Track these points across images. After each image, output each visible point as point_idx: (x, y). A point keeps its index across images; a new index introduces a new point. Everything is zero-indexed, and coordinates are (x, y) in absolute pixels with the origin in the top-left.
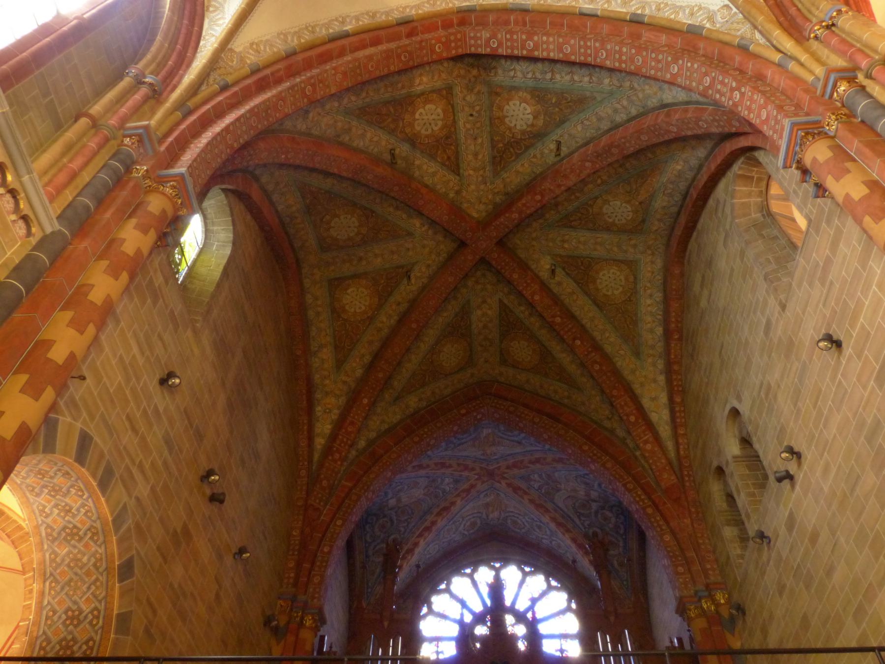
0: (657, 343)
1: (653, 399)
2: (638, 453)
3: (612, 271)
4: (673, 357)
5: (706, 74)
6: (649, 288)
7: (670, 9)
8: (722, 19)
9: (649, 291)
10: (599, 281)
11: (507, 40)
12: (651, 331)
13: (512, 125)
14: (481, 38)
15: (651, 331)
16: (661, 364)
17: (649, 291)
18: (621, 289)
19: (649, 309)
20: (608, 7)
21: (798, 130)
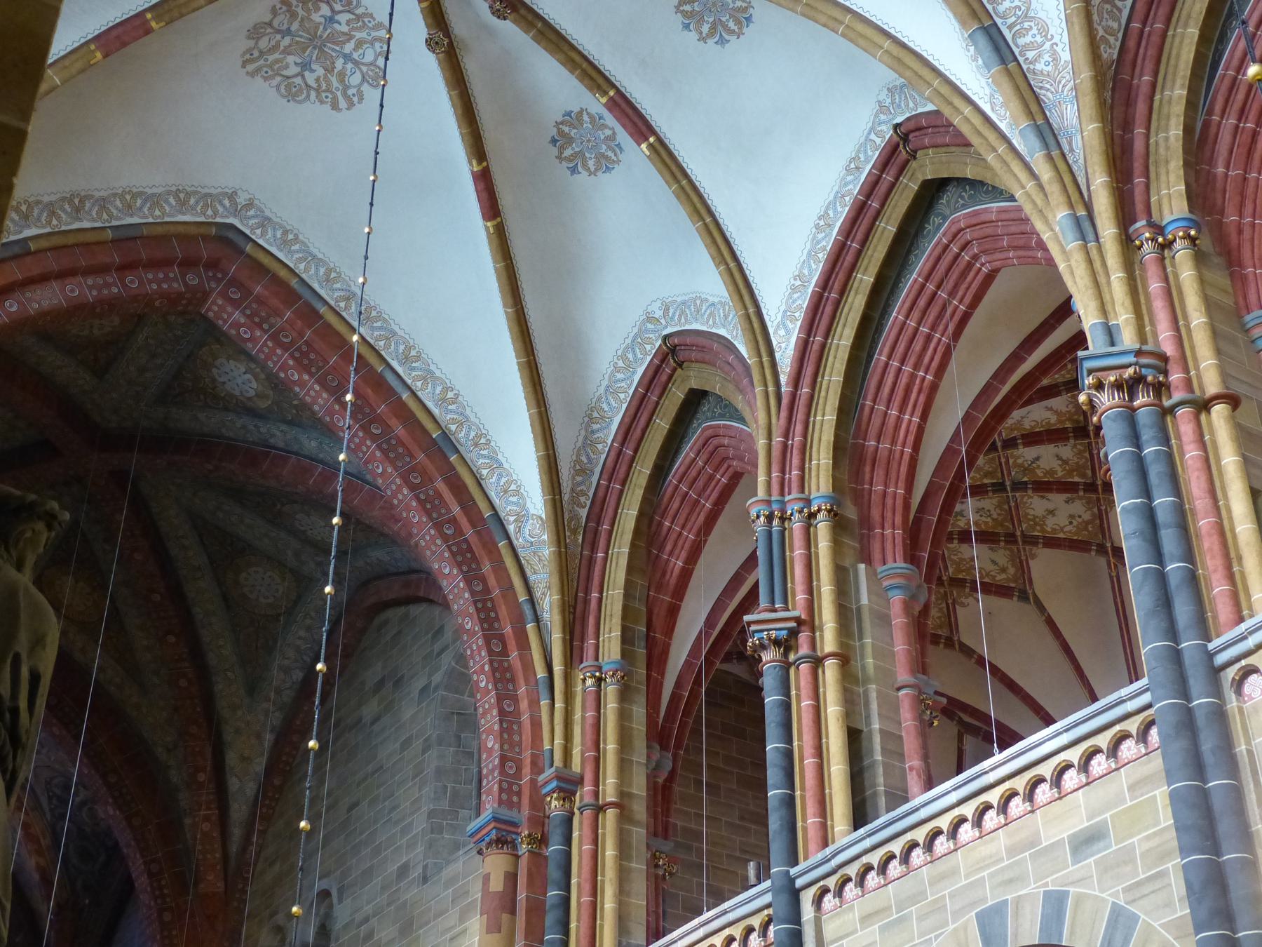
0: (286, 689)
1: (245, 759)
2: (188, 821)
3: (269, 573)
4: (298, 722)
5: (470, 616)
6: (312, 618)
7: (488, 457)
8: (529, 535)
9: (308, 621)
10: (244, 575)
11: (265, 344)
12: (286, 670)
13: (221, 380)
14: (230, 315)
15: (286, 670)
16: (276, 718)
17: (308, 621)
18: (271, 600)
19: (299, 642)
20: (421, 389)
21: (494, 828)
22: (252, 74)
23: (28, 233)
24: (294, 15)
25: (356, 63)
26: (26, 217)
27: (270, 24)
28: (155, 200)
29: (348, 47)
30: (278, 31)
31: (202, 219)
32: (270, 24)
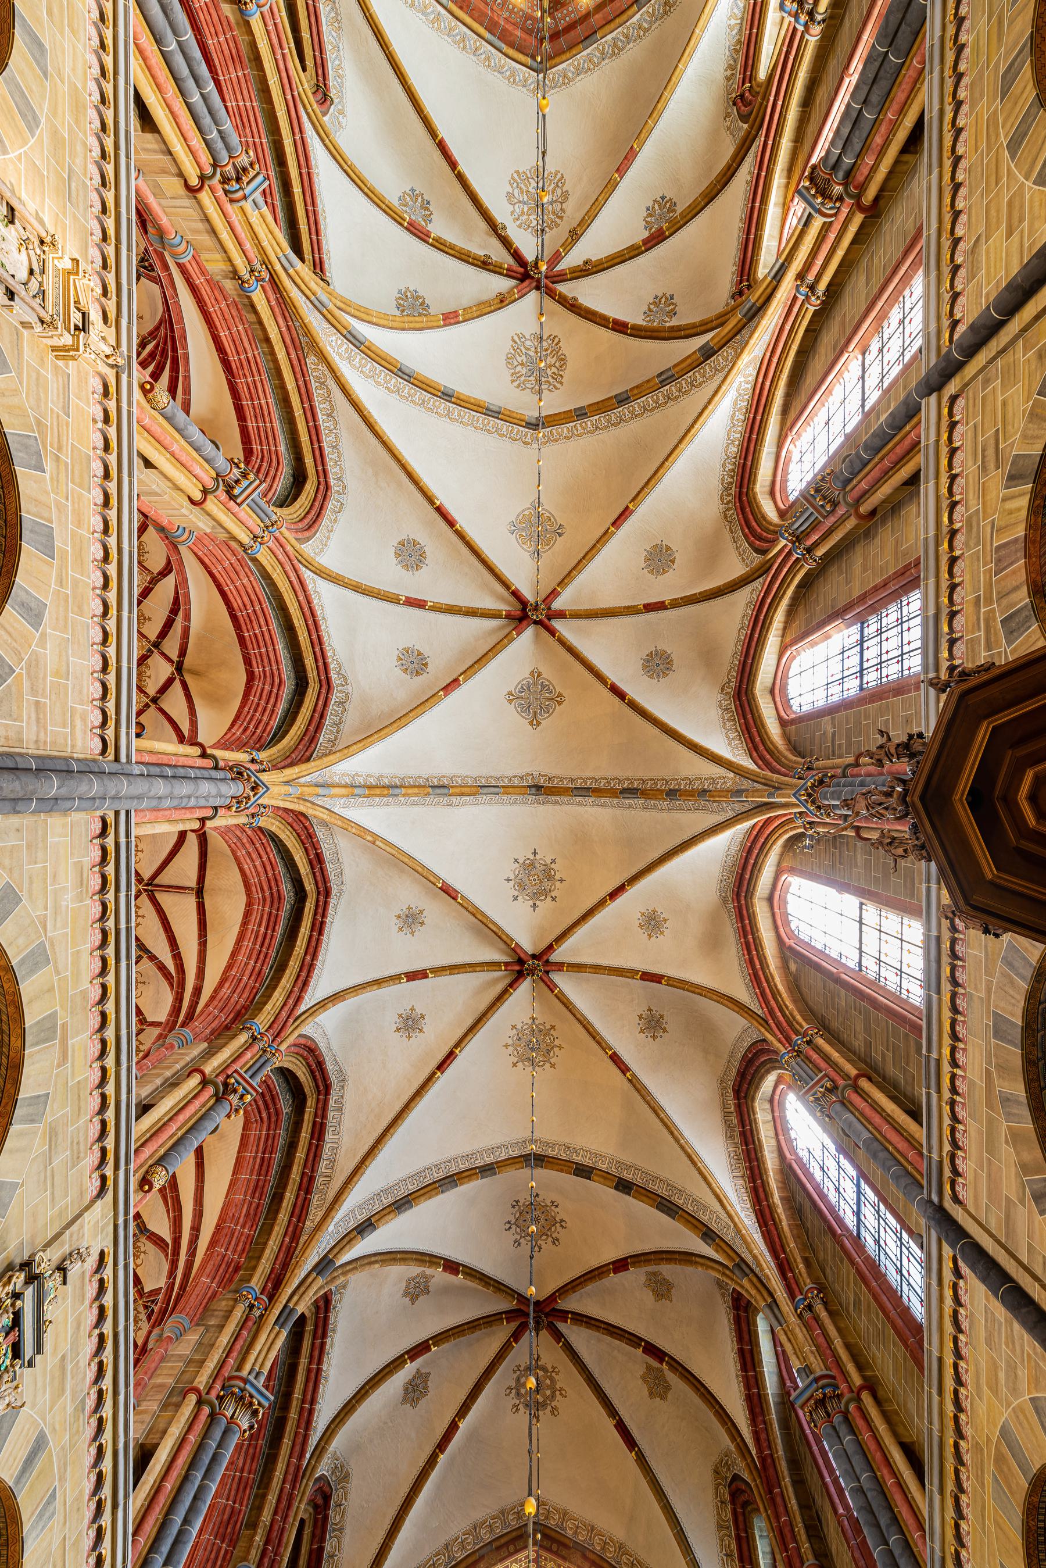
22: (557, 172)
23: (638, 16)
24: (554, 213)
25: (520, 202)
26: (640, 27)
27: (562, 203)
28: (579, 71)
29: (526, 210)
30: (556, 201)
31: (553, 70)
32: (562, 203)
